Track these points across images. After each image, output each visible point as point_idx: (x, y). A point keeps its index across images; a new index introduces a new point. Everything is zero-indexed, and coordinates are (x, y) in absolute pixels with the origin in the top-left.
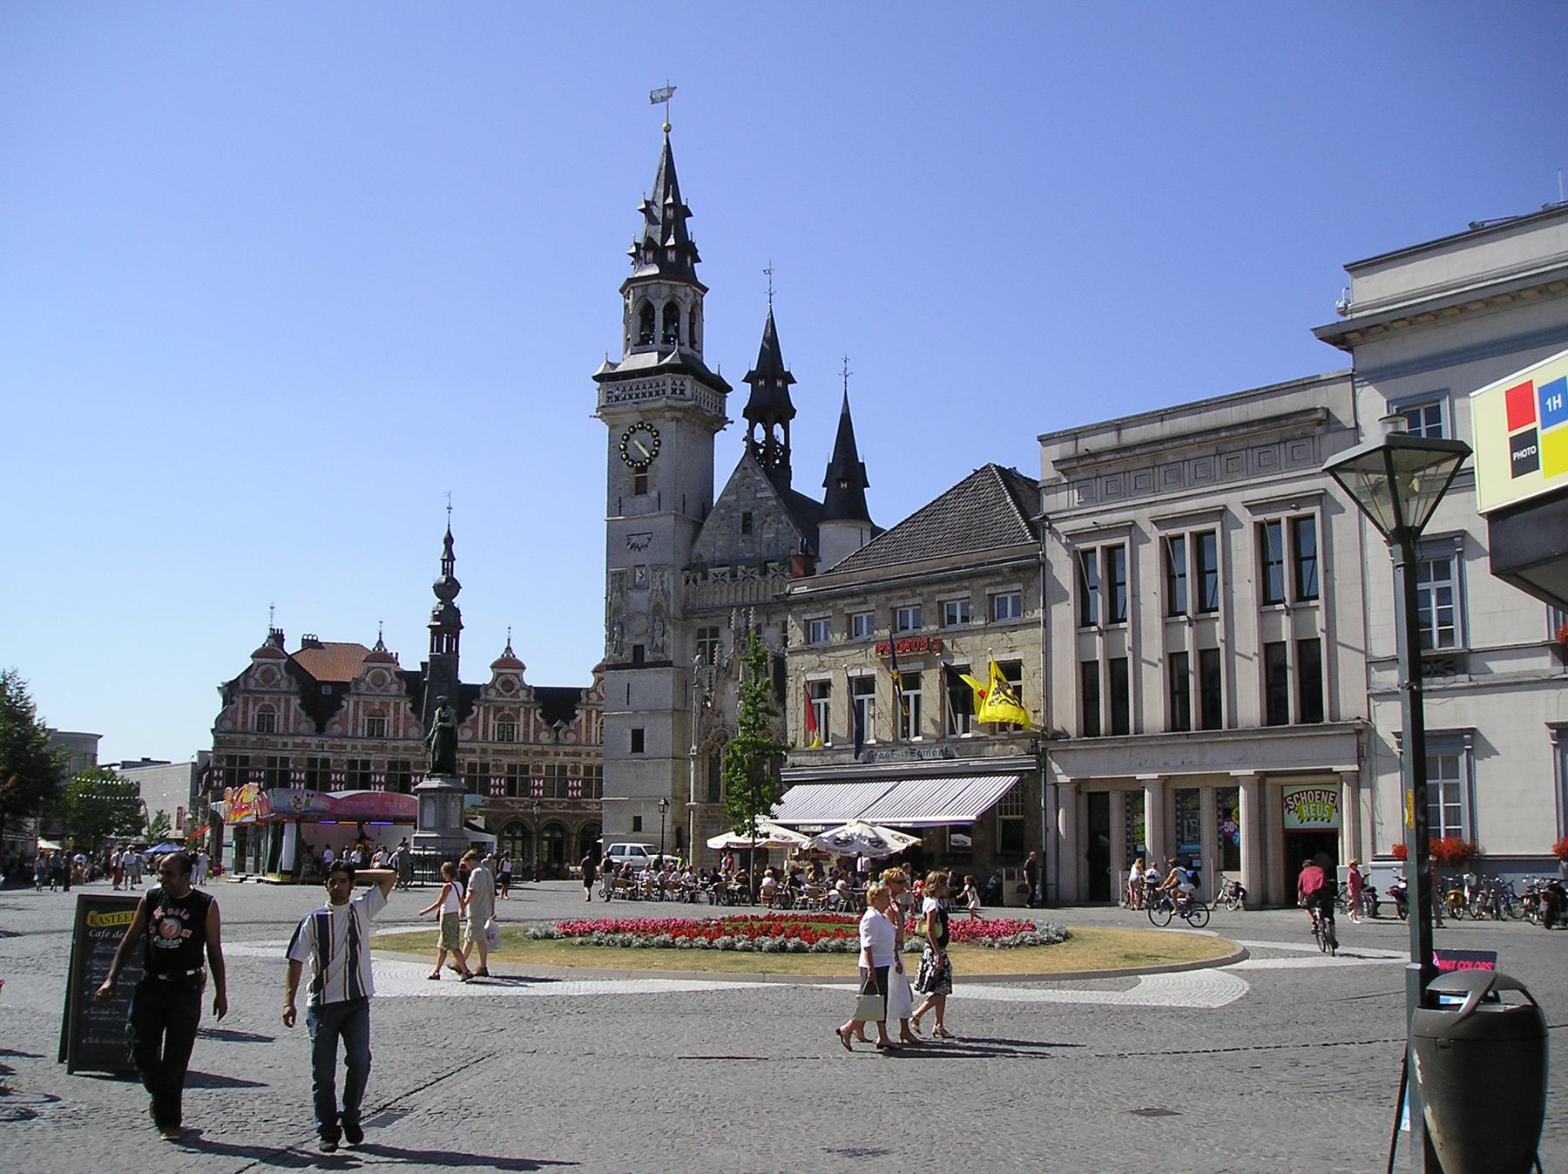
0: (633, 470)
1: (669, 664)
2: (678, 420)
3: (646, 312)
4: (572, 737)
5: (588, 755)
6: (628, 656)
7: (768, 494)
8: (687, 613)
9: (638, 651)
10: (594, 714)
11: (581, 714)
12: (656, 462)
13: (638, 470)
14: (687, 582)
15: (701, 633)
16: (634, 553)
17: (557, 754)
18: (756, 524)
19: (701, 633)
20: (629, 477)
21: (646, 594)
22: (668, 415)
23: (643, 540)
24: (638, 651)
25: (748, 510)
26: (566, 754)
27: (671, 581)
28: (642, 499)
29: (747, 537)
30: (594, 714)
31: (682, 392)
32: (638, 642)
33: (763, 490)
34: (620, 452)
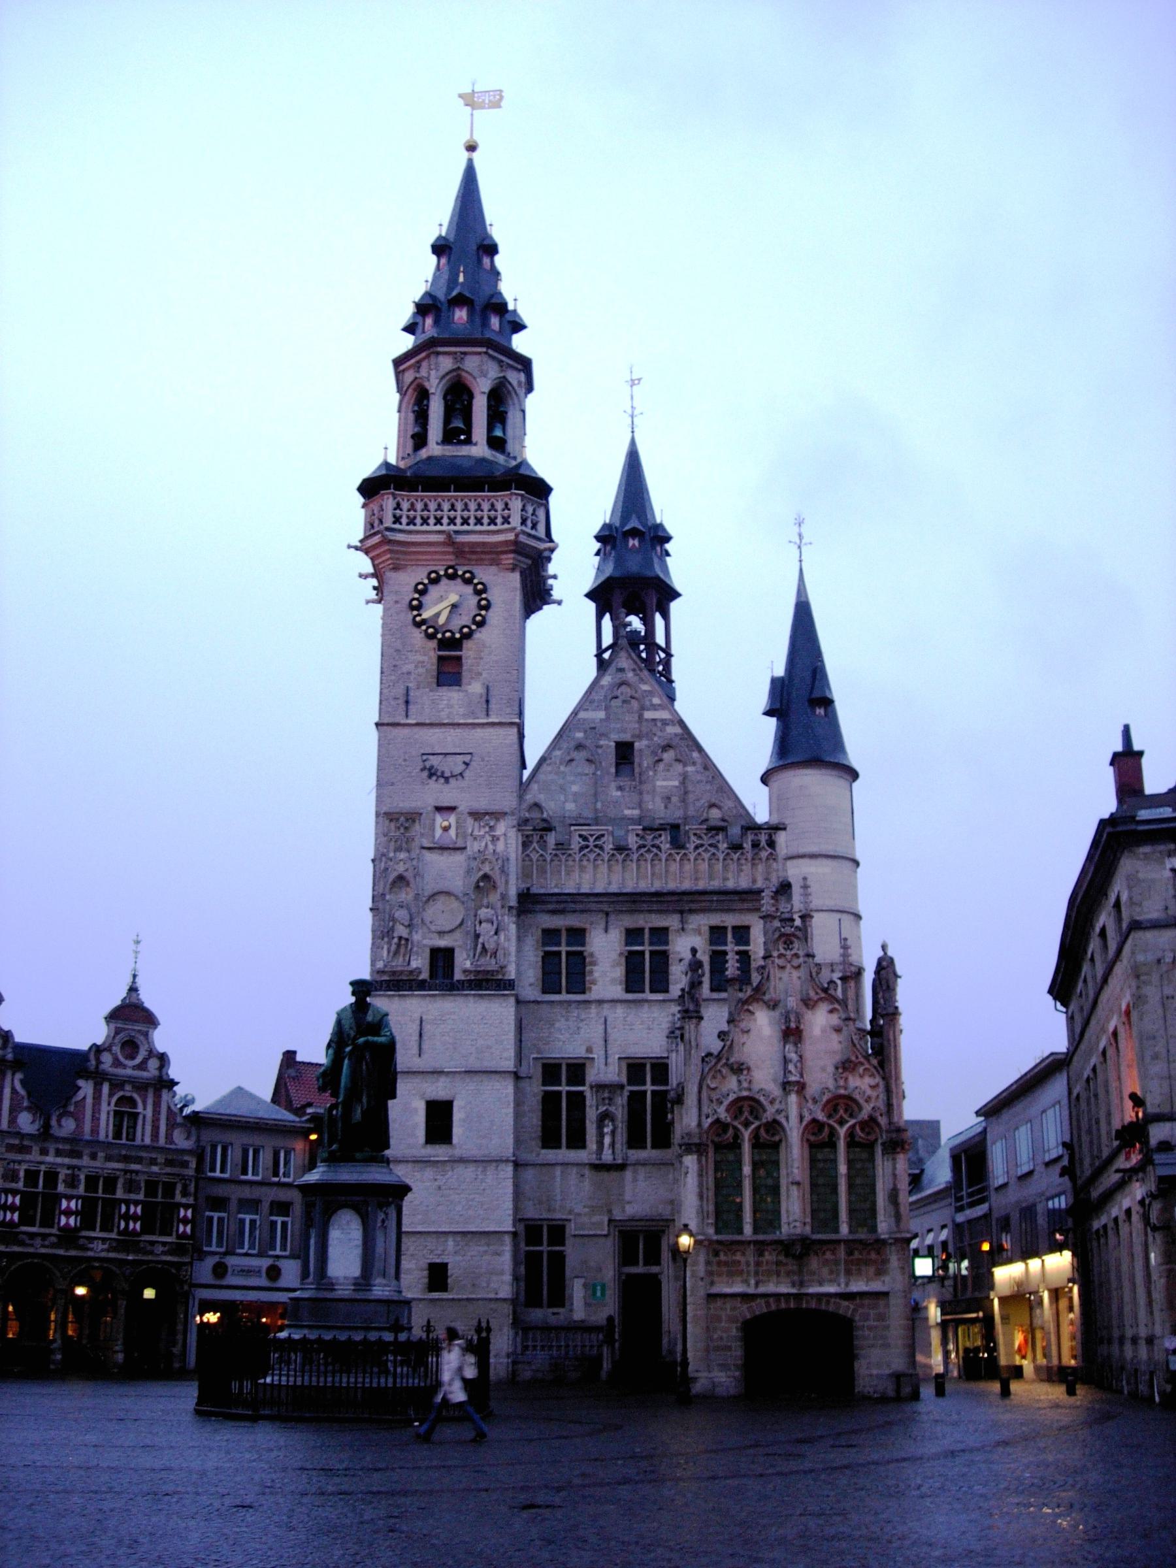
0: (433, 644)
1: (510, 985)
2: (522, 573)
3: (458, 395)
4: (69, 1125)
5: (93, 1157)
6: (420, 963)
7: (665, 715)
8: (528, 903)
9: (442, 958)
10: (106, 1088)
11: (86, 1088)
12: (481, 635)
13: (444, 644)
14: (525, 845)
15: (550, 935)
16: (434, 785)
17: (44, 1152)
18: (643, 760)
19: (550, 935)
20: (425, 654)
21: (459, 858)
22: (508, 559)
23: (455, 764)
24: (442, 958)
25: (627, 737)
26: (58, 1153)
27: (507, 840)
28: (450, 696)
29: (625, 781)
30: (106, 1088)
31: (534, 526)
32: (443, 943)
33: (655, 708)
34: (408, 615)
